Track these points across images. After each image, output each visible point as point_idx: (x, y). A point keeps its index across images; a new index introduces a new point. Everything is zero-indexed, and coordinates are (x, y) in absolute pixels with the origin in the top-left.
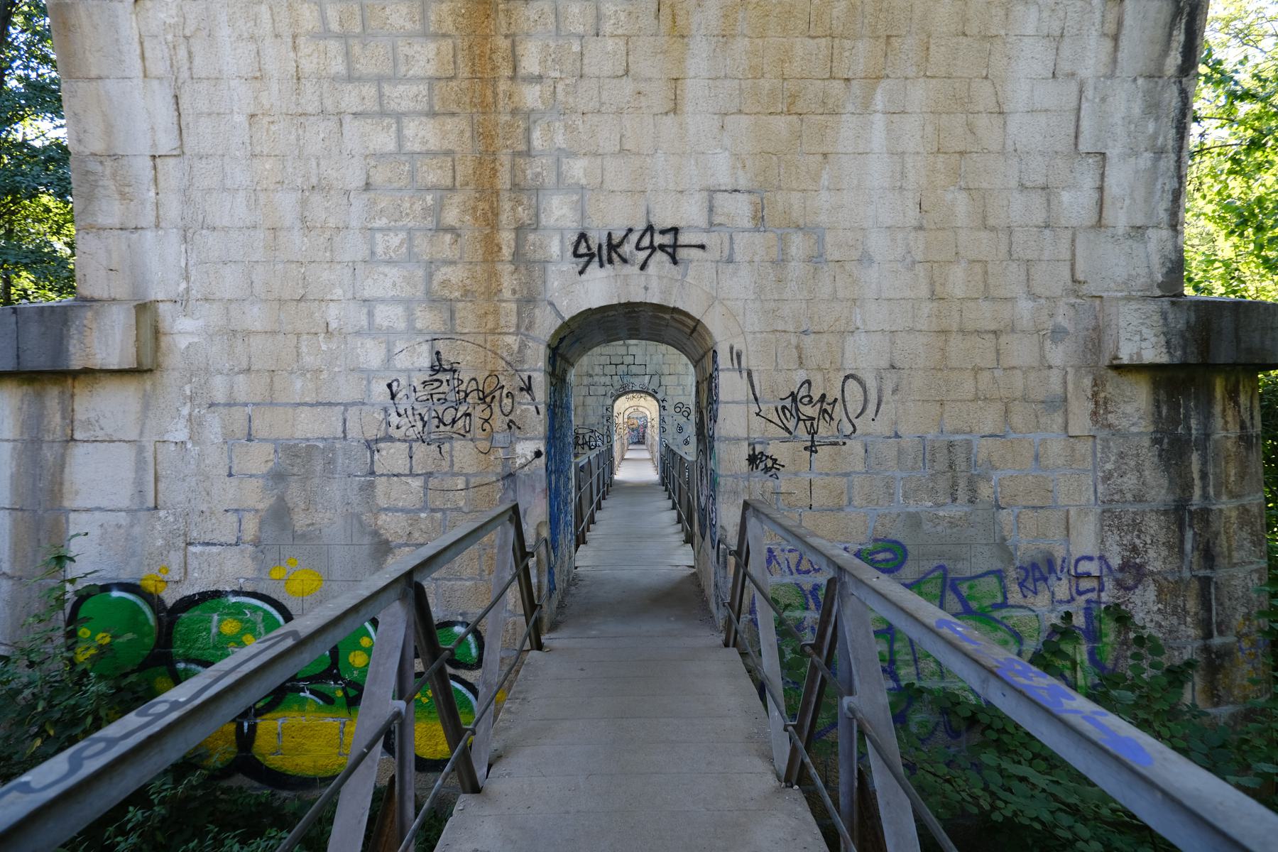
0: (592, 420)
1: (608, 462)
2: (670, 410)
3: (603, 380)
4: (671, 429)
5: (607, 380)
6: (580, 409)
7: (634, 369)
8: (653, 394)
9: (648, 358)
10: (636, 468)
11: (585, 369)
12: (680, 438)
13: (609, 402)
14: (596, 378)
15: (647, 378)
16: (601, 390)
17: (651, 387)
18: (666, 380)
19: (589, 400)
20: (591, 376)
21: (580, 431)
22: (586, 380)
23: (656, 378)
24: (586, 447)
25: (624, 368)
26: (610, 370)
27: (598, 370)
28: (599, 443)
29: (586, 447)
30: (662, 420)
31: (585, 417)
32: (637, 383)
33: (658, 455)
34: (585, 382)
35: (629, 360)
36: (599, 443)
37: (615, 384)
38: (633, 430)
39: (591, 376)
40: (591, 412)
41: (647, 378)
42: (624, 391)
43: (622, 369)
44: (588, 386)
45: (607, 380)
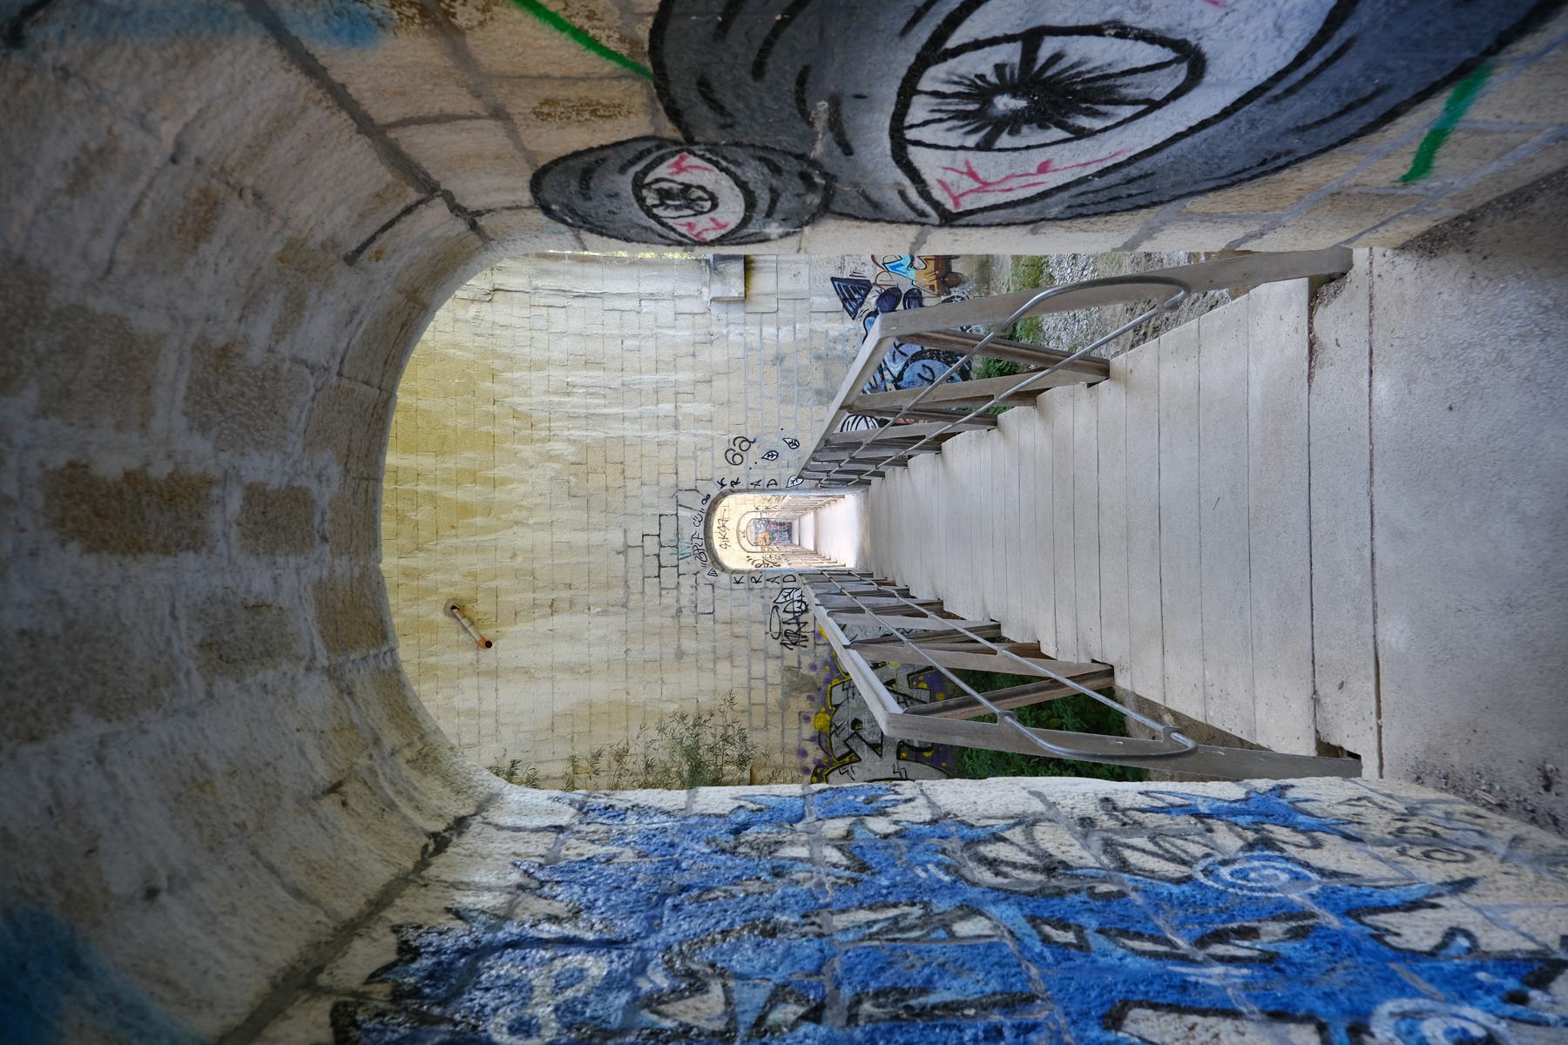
0: (756, 607)
1: (828, 579)
2: (737, 472)
3: (686, 590)
4: (771, 471)
5: (687, 582)
6: (738, 630)
7: (668, 536)
8: (713, 504)
9: (649, 511)
10: (837, 532)
11: (668, 621)
12: (787, 455)
13: (724, 579)
14: (685, 601)
15: (682, 512)
16: (705, 593)
17: (699, 506)
18: (687, 480)
19: (722, 613)
20: (680, 611)
21: (776, 628)
22: (688, 619)
23: (685, 498)
24: (803, 618)
25: (665, 553)
26: (669, 576)
27: (669, 599)
28: (796, 595)
29: (803, 618)
30: (755, 487)
31: (752, 621)
32: (691, 530)
33: (814, 497)
34: (691, 620)
35: (651, 544)
36: (796, 595)
37: (694, 568)
38: (772, 539)
39: (680, 611)
40: (743, 611)
41: (682, 512)
42: (706, 552)
43: (667, 557)
44: (697, 614)
45: (687, 582)
